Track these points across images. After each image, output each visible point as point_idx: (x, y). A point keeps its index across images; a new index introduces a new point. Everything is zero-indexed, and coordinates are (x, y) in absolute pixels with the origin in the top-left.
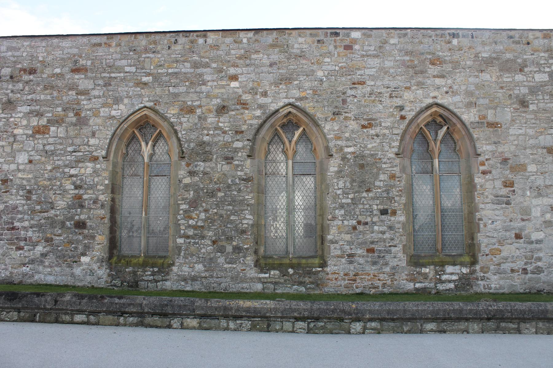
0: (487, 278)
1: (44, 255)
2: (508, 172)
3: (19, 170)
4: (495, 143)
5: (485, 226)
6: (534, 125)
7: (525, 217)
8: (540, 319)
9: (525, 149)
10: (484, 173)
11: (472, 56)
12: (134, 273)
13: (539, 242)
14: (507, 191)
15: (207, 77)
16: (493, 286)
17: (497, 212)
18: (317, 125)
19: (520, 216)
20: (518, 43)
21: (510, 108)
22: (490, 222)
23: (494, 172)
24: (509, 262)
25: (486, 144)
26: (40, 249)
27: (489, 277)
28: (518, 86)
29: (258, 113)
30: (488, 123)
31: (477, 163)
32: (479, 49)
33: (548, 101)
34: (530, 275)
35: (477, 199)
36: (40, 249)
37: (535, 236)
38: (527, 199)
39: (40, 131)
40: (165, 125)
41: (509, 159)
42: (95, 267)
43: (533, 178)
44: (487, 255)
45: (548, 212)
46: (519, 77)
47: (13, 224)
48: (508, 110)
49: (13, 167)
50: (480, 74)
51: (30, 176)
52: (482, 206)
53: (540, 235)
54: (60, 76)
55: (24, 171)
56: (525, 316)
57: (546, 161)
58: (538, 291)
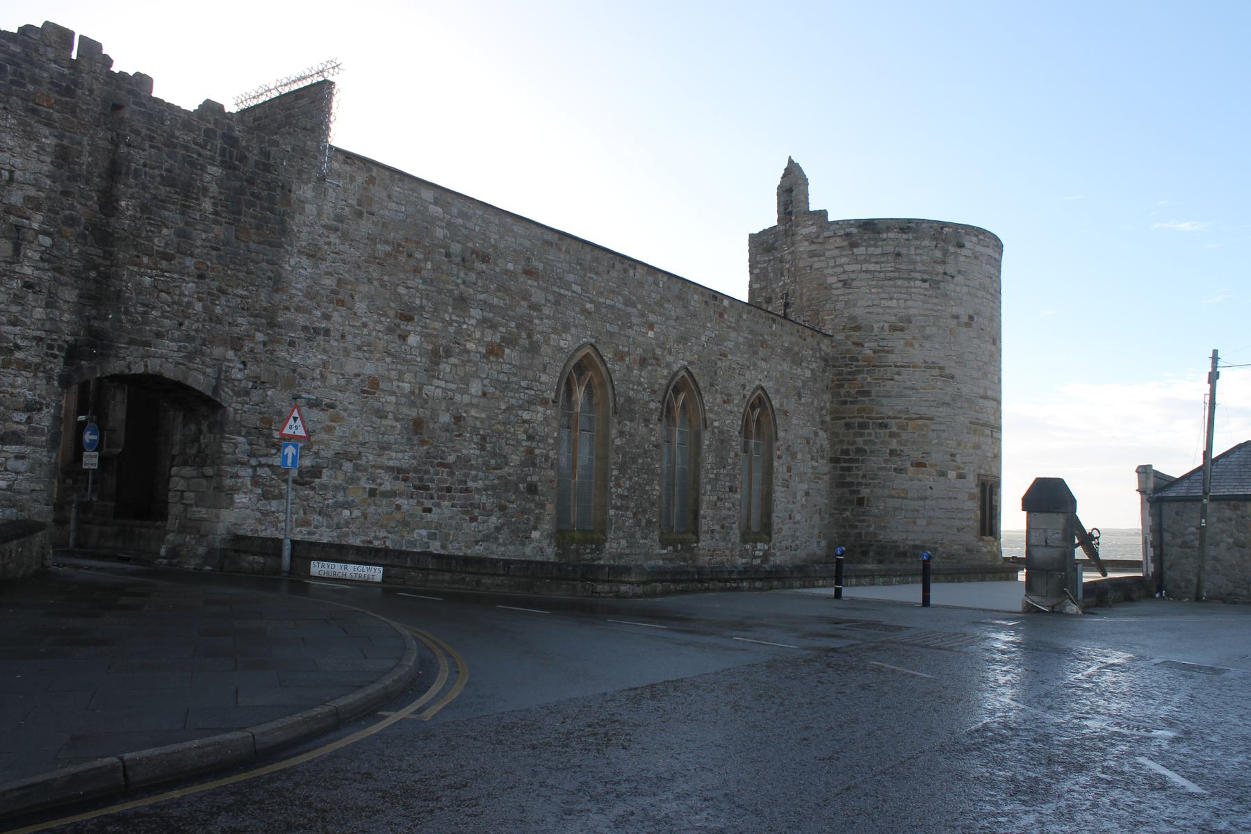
1: (498, 529)
3: (472, 405)
12: (577, 550)
15: (634, 320)
18: (700, 394)
26: (494, 520)
29: (665, 372)
36: (494, 520)
39: (493, 351)
40: (602, 369)
42: (545, 543)
47: (465, 482)
49: (466, 399)
51: (484, 415)
54: (513, 275)
55: (477, 406)
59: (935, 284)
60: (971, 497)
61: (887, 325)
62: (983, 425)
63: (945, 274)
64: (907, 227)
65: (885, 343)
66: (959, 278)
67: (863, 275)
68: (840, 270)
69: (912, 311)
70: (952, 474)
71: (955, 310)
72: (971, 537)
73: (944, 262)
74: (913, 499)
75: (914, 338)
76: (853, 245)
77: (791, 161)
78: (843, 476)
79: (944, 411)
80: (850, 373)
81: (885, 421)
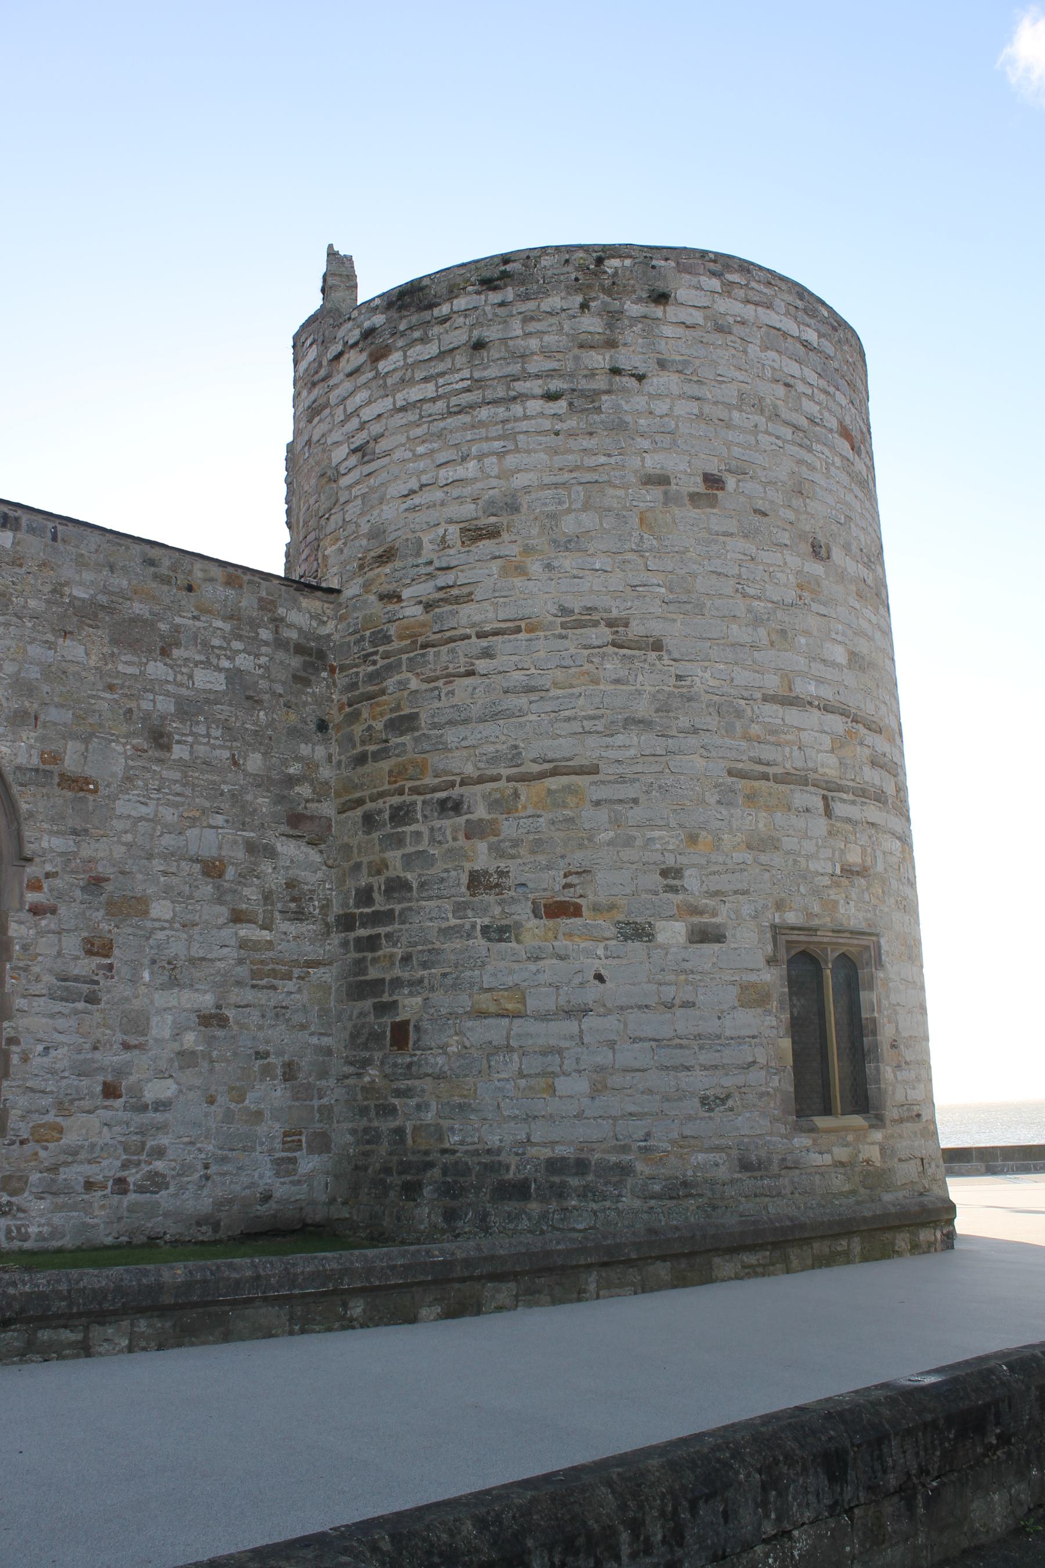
0: (19, 1210)
2: (101, 913)
4: (75, 832)
5: (25, 1059)
6: (177, 799)
7: (133, 1041)
8: (141, 1311)
9: (150, 857)
10: (36, 910)
11: (47, 589)
13: (161, 1106)
14: (93, 966)
16: (33, 1230)
17: (61, 1023)
19: (119, 1037)
20: (166, 580)
21: (124, 745)
22: (40, 1048)
23: (62, 910)
24: (81, 1163)
25: (51, 833)
27: (25, 1205)
28: (151, 691)
30: (62, 775)
31: (21, 883)
32: (68, 572)
33: (217, 742)
34: (132, 1197)
35: (10, 982)
37: (156, 1090)
38: (142, 990)
41: (108, 880)
43: (161, 935)
44: (22, 1142)
45: (188, 1028)
46: (157, 669)
48: (119, 748)
50: (60, 641)
52: (20, 1003)
53: (166, 1089)
56: (106, 1306)
57: (197, 894)
58: (149, 1238)
59: (585, 401)
60: (753, 997)
61: (454, 530)
62: (784, 779)
63: (615, 371)
64: (497, 274)
65: (448, 578)
66: (660, 381)
67: (399, 419)
68: (355, 423)
69: (520, 480)
70: (672, 932)
71: (653, 463)
72: (759, 1121)
73: (611, 344)
74: (544, 1017)
75: (528, 550)
76: (376, 357)
77: (332, 254)
78: (360, 966)
79: (633, 741)
80: (371, 677)
81: (456, 792)
